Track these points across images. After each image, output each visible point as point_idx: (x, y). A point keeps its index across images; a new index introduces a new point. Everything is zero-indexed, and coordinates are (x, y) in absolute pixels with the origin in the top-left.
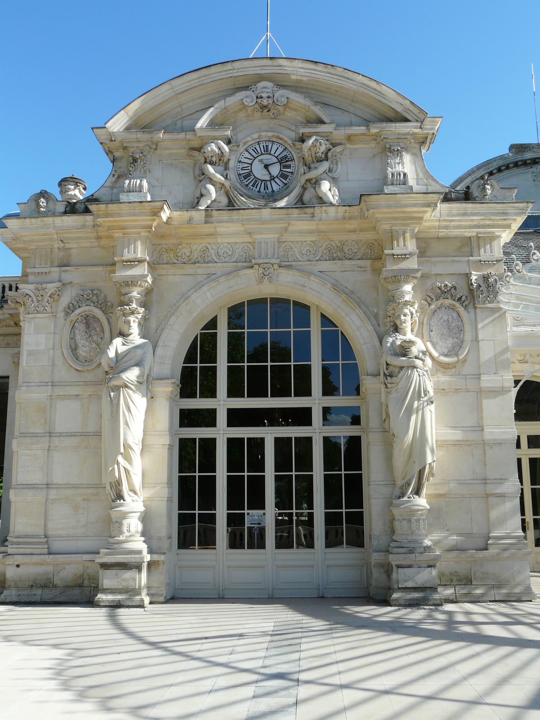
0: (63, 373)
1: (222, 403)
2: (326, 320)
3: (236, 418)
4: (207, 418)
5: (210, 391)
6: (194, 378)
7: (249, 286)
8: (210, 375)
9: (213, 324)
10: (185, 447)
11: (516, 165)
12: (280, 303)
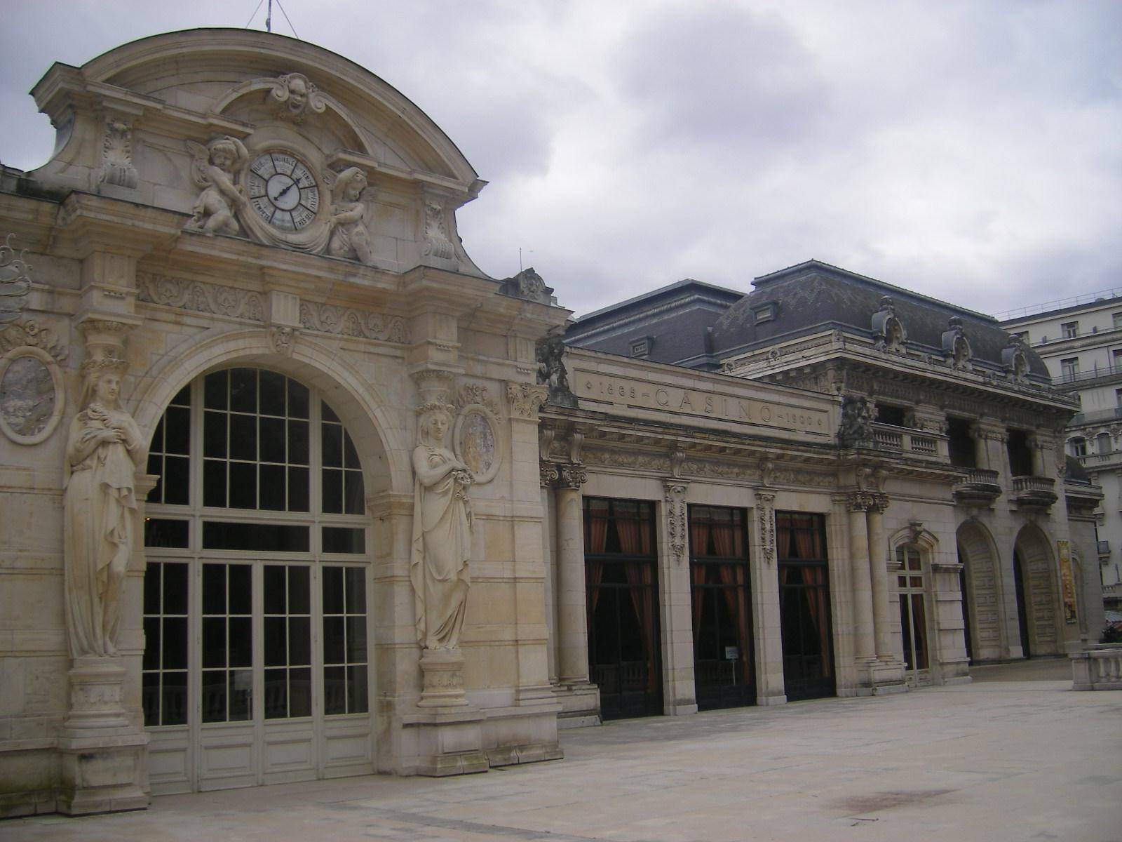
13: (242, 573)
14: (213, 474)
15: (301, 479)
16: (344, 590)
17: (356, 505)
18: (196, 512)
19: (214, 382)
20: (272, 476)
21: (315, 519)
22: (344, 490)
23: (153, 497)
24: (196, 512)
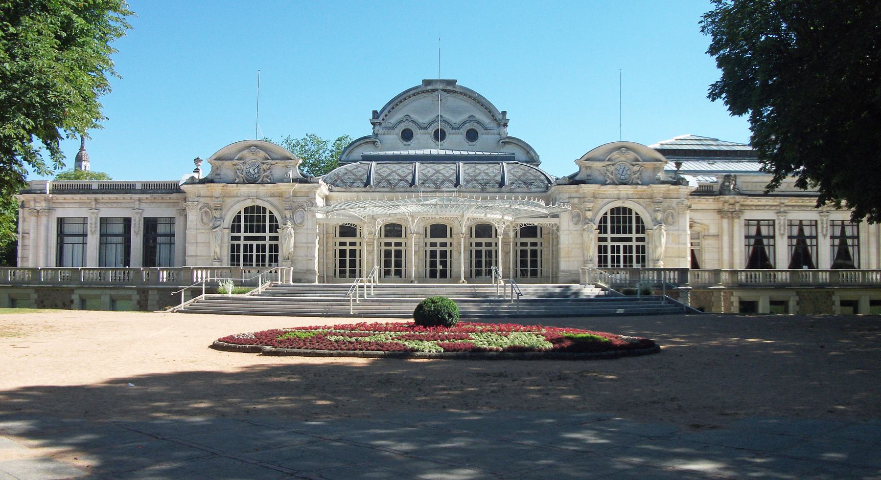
0: (200, 227)
1: (242, 234)
2: (271, 212)
3: (246, 238)
4: (238, 238)
5: (239, 231)
6: (235, 228)
7: (249, 203)
8: (239, 227)
9: (240, 212)
10: (233, 246)
11: (423, 92)
12: (258, 207)
13: (618, 247)
14: (612, 228)
15: (631, 228)
16: (642, 250)
17: (643, 232)
18: (609, 235)
19: (612, 210)
20: (624, 228)
21: (634, 236)
22: (641, 229)
23: (600, 233)
24: (609, 235)
